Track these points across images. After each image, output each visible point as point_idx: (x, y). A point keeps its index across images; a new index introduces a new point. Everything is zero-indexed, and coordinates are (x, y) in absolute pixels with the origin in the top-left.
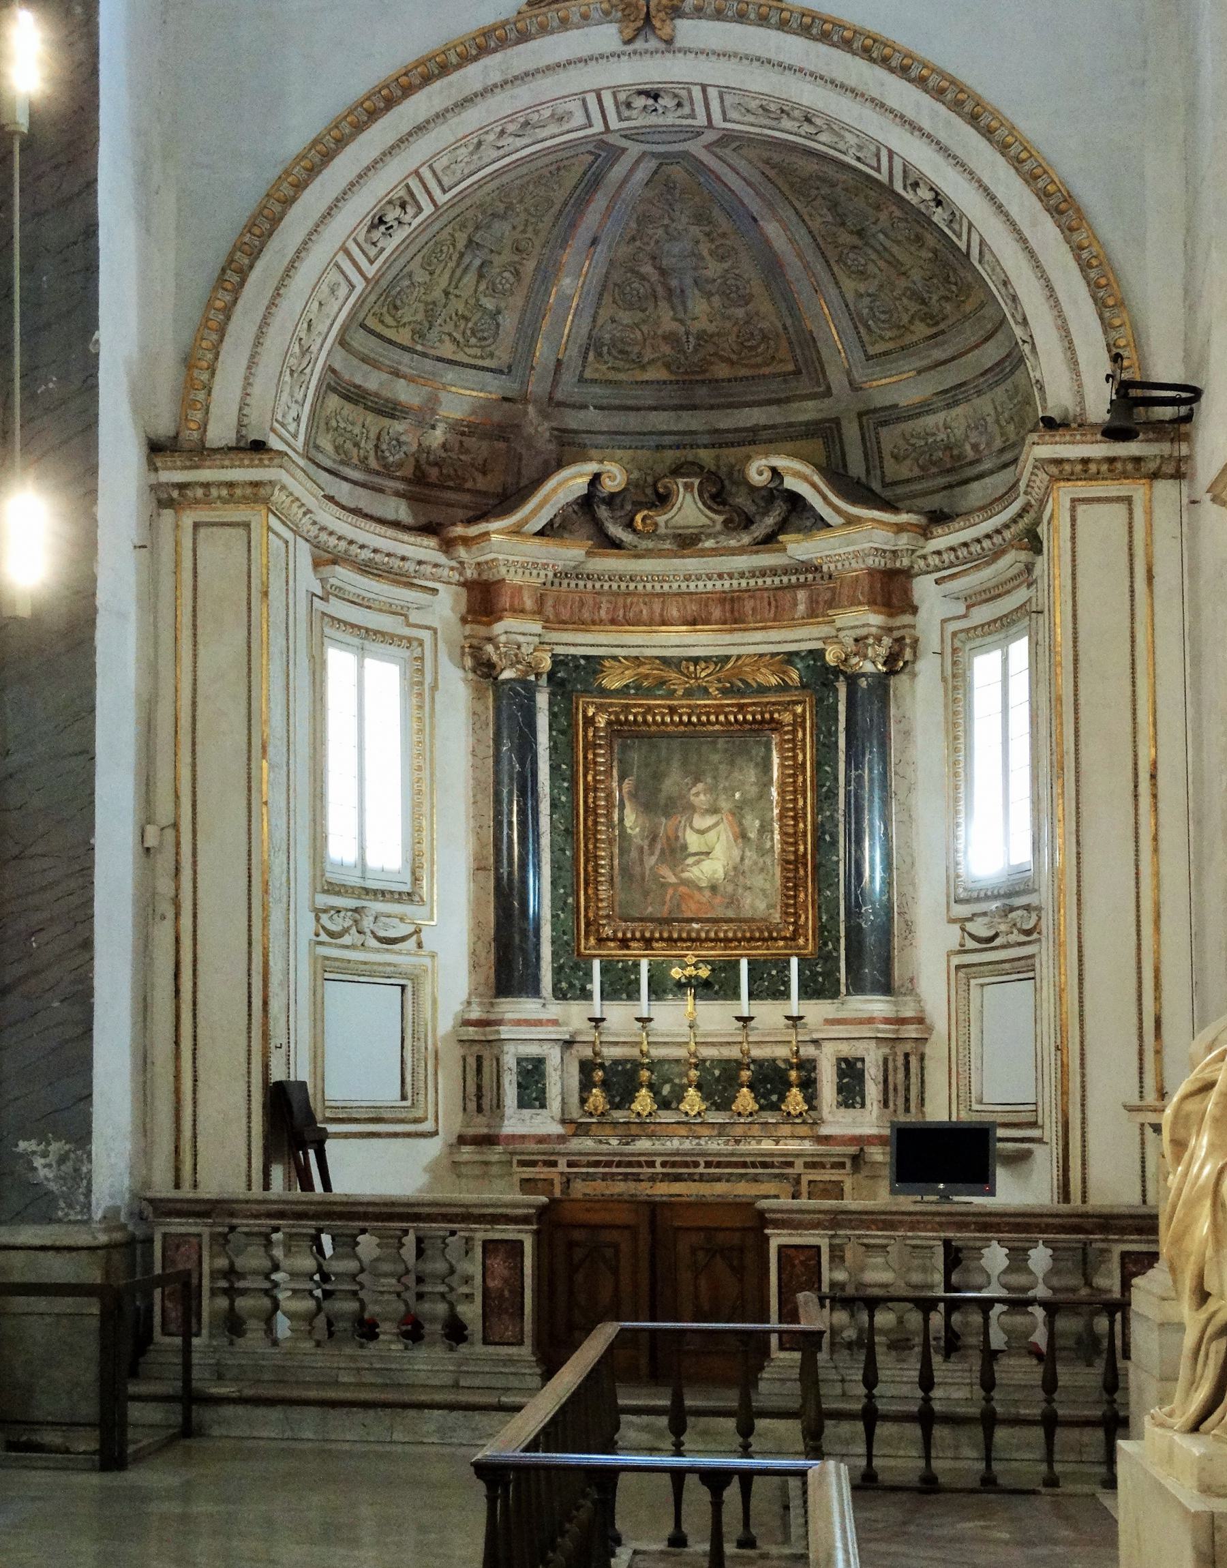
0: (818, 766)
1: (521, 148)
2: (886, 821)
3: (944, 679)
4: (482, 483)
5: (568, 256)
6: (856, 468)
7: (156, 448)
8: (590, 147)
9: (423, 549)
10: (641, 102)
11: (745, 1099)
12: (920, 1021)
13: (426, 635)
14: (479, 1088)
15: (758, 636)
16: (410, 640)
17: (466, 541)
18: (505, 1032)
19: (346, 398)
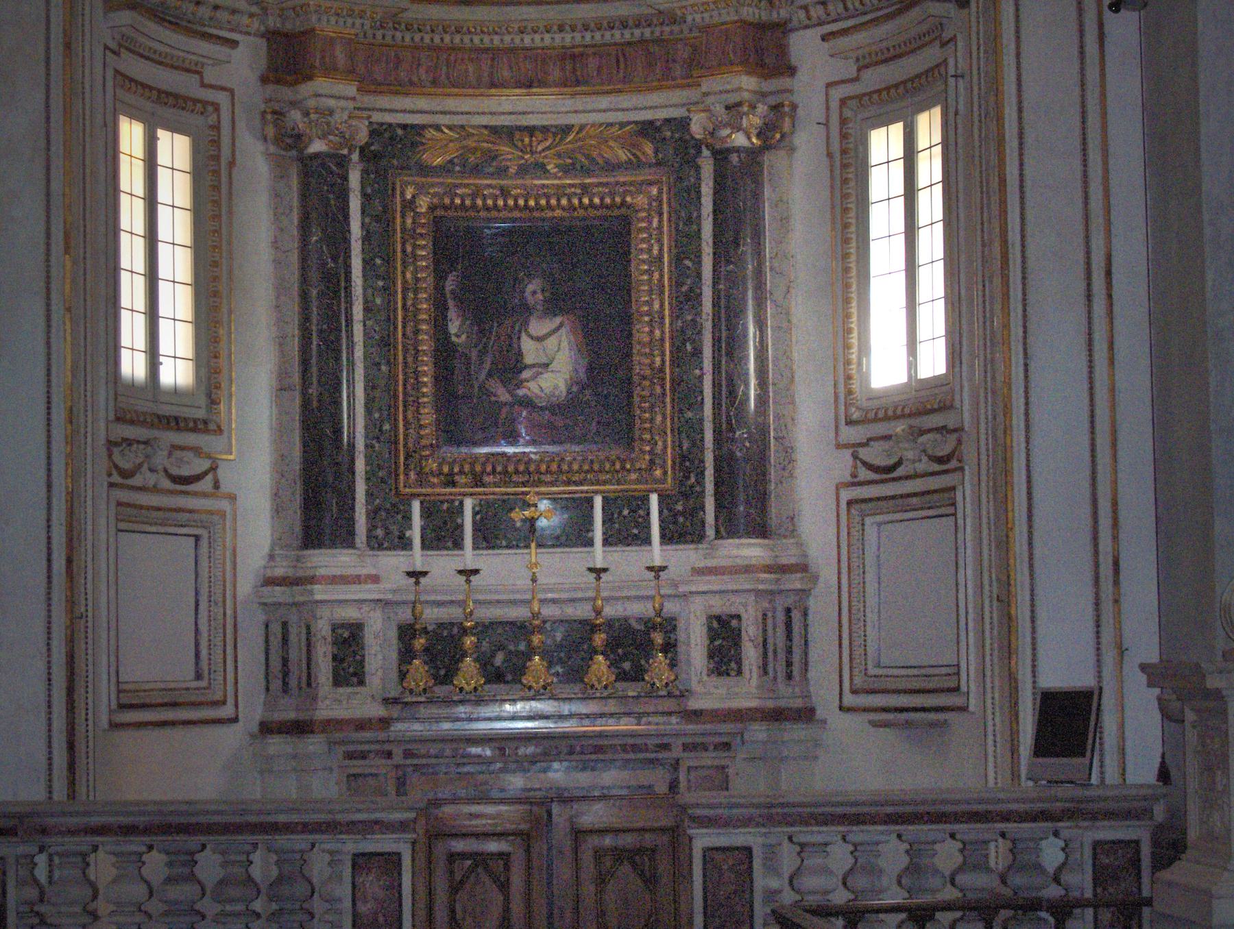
2: (761, 324)
3: (830, 155)
12: (803, 568)
14: (285, 661)
15: (604, 102)
16: (205, 103)
18: (320, 592)
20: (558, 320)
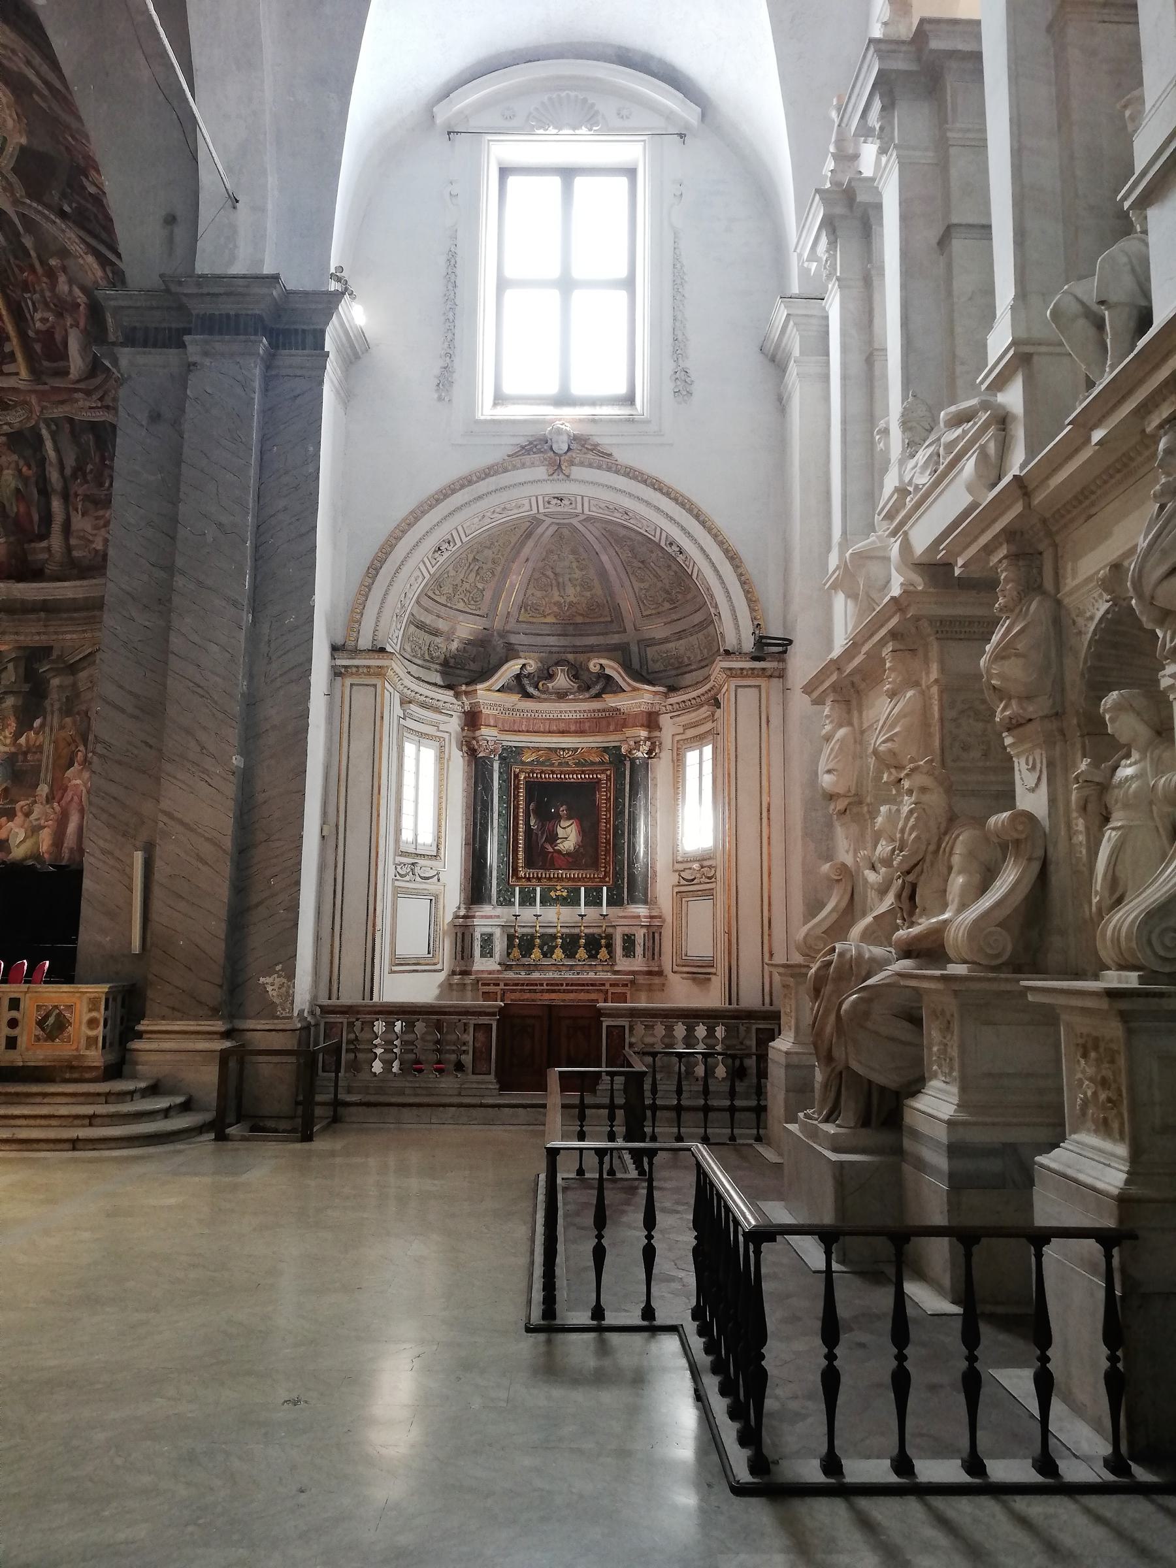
0: (616, 799)
1: (501, 519)
3: (673, 761)
4: (473, 666)
5: (515, 566)
6: (636, 664)
7: (335, 649)
8: (530, 519)
9: (447, 696)
10: (554, 501)
11: (582, 953)
13: (446, 735)
14: (463, 948)
15: (591, 739)
16: (439, 737)
17: (466, 693)
19: (417, 627)
20: (571, 821)
